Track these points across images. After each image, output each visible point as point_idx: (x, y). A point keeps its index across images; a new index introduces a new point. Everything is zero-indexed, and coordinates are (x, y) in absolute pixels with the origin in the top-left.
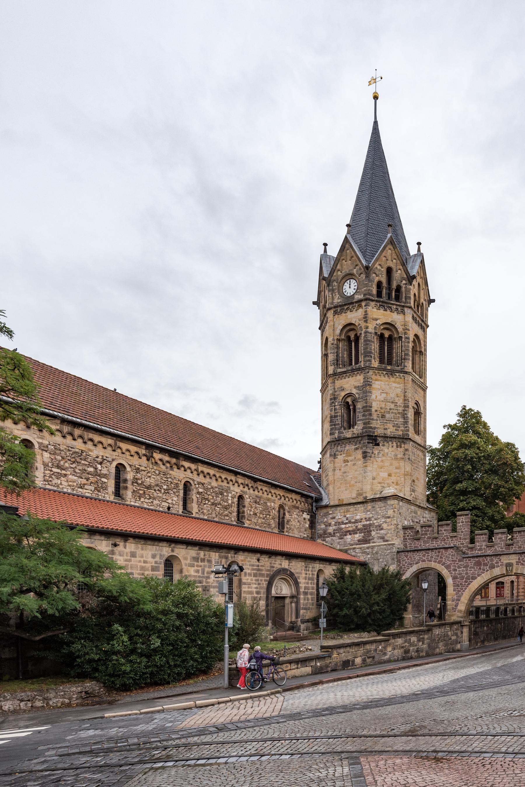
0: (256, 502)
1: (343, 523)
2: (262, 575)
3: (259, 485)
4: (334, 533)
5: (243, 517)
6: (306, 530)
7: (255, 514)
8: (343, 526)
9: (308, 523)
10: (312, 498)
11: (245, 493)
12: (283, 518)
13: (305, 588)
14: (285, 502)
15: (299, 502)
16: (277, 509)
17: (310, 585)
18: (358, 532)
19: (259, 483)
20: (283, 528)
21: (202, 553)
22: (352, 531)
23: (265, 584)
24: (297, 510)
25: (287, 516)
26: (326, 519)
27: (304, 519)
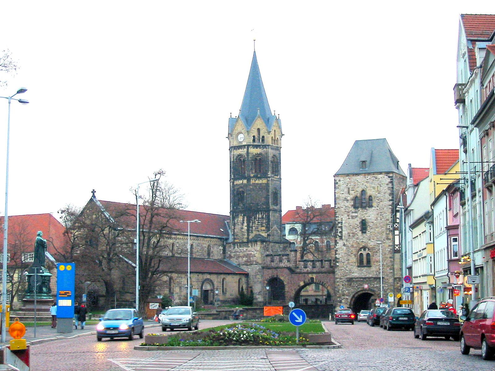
0: (198, 246)
2: (200, 282)
3: (199, 238)
5: (193, 253)
6: (221, 255)
7: (197, 251)
8: (238, 253)
9: (222, 251)
10: (224, 239)
11: (193, 243)
12: (210, 251)
13: (217, 286)
14: (211, 243)
15: (217, 242)
16: (207, 247)
17: (219, 285)
19: (199, 237)
20: (210, 255)
21: (179, 275)
23: (200, 285)
24: (217, 246)
25: (212, 249)
27: (220, 249)
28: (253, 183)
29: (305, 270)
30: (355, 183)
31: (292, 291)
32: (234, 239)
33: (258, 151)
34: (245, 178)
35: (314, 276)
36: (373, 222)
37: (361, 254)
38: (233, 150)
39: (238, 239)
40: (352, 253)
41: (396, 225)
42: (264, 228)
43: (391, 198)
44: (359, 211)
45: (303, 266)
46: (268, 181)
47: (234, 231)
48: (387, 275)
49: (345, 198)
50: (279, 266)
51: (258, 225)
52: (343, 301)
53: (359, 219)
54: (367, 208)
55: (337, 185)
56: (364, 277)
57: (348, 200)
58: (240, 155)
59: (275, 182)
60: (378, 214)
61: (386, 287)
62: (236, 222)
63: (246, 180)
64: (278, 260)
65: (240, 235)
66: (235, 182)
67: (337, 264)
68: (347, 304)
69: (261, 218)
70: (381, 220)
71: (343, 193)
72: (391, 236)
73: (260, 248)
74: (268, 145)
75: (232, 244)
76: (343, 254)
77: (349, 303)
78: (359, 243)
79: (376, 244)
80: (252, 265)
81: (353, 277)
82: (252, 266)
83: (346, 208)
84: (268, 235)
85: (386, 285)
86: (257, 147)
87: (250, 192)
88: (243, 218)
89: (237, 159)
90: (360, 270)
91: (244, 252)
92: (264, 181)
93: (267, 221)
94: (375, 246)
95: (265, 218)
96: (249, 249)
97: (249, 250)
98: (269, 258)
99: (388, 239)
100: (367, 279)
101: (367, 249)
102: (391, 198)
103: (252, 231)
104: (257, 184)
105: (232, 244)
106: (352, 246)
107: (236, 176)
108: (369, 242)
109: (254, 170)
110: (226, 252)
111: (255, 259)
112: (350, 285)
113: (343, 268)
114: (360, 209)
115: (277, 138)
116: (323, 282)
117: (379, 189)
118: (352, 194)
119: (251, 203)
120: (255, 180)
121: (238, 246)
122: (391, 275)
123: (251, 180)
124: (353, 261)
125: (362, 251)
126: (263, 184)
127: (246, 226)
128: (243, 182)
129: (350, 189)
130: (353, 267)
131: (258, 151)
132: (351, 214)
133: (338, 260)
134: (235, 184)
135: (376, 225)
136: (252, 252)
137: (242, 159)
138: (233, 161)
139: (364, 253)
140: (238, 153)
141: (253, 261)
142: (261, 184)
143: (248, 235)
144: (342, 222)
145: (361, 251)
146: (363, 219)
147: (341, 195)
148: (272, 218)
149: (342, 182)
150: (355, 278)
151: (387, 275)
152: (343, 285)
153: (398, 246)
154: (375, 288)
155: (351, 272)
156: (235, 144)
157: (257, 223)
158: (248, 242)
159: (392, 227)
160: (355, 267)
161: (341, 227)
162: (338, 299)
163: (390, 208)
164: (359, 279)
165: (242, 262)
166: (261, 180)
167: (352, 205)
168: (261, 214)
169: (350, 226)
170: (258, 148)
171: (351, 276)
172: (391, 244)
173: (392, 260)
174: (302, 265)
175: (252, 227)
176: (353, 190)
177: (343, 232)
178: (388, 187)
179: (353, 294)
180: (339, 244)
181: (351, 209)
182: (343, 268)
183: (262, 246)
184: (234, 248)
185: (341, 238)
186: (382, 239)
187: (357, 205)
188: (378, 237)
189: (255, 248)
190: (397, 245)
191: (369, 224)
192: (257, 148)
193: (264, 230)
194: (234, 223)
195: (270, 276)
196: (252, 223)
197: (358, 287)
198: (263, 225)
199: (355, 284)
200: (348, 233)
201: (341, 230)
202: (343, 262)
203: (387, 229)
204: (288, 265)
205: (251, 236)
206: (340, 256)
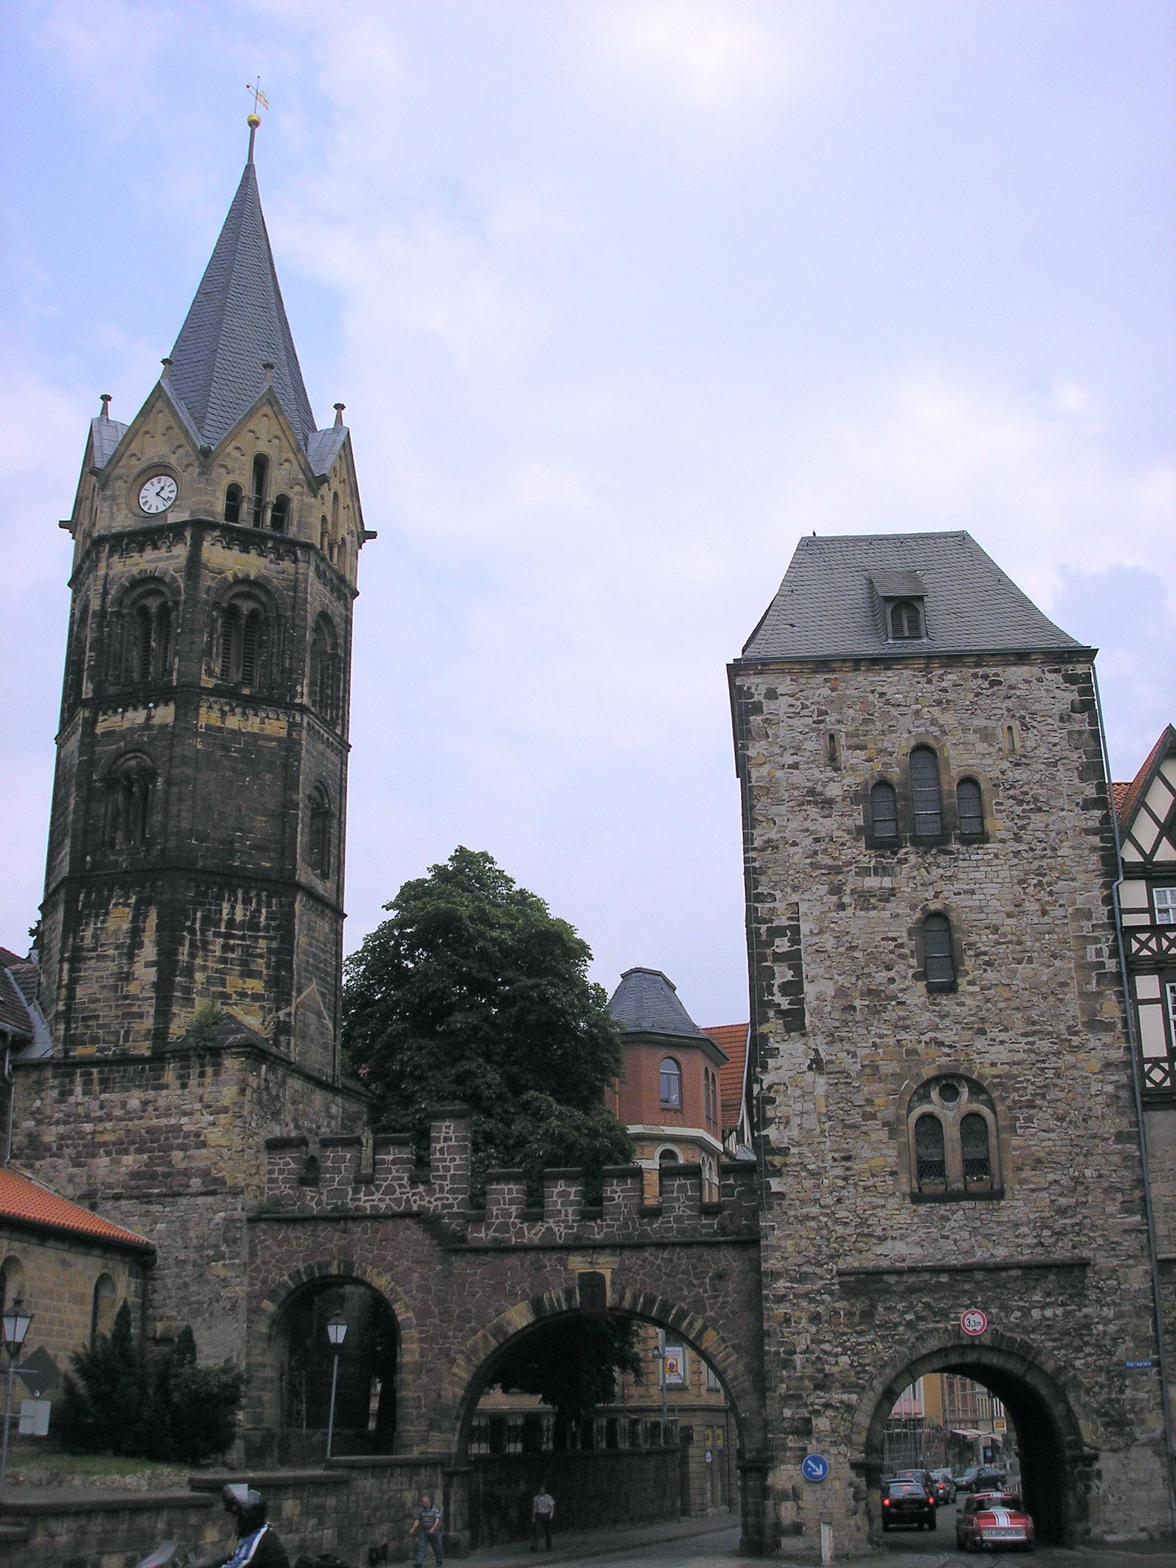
1: (88, 1118)
4: (60, 1148)
8: (88, 1127)
18: (132, 1148)
22: (114, 1144)
26: (38, 1103)
28: (208, 727)
29: (533, 1234)
30: (866, 707)
31: (453, 1362)
32: (71, 1041)
33: (251, 564)
34: (164, 695)
35: (606, 1266)
36: (996, 930)
37: (929, 1125)
38: (104, 555)
39: (94, 1040)
40: (873, 1117)
41: (1144, 945)
42: (256, 986)
43: (1090, 791)
44: (900, 862)
45: (513, 1209)
46: (292, 725)
47: (71, 996)
48: (1111, 1247)
49: (811, 792)
50: (351, 1205)
51: (224, 960)
52: (822, 1423)
53: (904, 910)
54: (955, 846)
55: (756, 720)
56: (952, 1261)
57: (829, 803)
58: (148, 583)
59: (321, 747)
60: (1023, 881)
61: (1106, 1321)
62: (88, 942)
63: (172, 707)
64: (346, 1170)
65: (107, 1013)
66: (101, 718)
67: (776, 1185)
68: (848, 1440)
69: (242, 926)
70: (1044, 913)
71: (789, 759)
72: (1110, 1009)
73: (242, 1092)
74: (308, 547)
75: (49, 1073)
76: (811, 1122)
77: (860, 1438)
78: (912, 1052)
79: (1022, 1056)
80: (179, 1195)
81: (885, 1263)
82: (183, 1201)
83: (817, 847)
84: (283, 1029)
85: (1108, 1312)
86: (245, 540)
87: (188, 771)
88: (139, 915)
89: (127, 602)
90: (927, 1220)
91: (129, 1116)
92: (274, 726)
93: (274, 945)
94: (1015, 1070)
95: (267, 928)
96: (169, 1096)
97: (162, 1102)
98: (289, 1161)
99: (1094, 1024)
100: (979, 1276)
101: (965, 1092)
102: (1090, 791)
103: (188, 991)
104: (233, 732)
105: (49, 1073)
106: (872, 1070)
107: (112, 690)
108: (980, 1043)
109: (220, 661)
110: (12, 1116)
111: (201, 1158)
112: (868, 1315)
113: (815, 1210)
114: (906, 850)
115: (343, 539)
116: (665, 1308)
117: (1018, 745)
118: (853, 769)
119: (191, 833)
120: (224, 714)
121: (88, 1083)
122: (1130, 1243)
123: (203, 710)
124: (880, 1162)
125: (935, 1104)
126: (269, 738)
127: (148, 965)
128: (149, 717)
129: (843, 740)
130: (882, 1202)
131: (251, 564)
132: (852, 881)
133: (777, 1160)
134: (100, 729)
135: (1019, 943)
136: (184, 1120)
137: (153, 604)
138: (102, 614)
139: (950, 1114)
140: (135, 571)
141: (187, 1173)
142: (255, 734)
143: (163, 1014)
144: (796, 930)
145: (925, 1098)
146: (934, 906)
147: (779, 774)
148: (301, 940)
149: (791, 700)
150: (899, 1272)
151: (1111, 1247)
152: (815, 1318)
153: (1166, 1065)
154: (1034, 1330)
155: (871, 1235)
156: (122, 522)
157: (217, 946)
158: (158, 1059)
159: (1114, 953)
160: (893, 1203)
161: (793, 959)
162: (787, 1413)
163: (1093, 849)
164: (926, 1277)
165: (112, 1179)
166: (256, 715)
167: (859, 829)
168: (247, 901)
169: (853, 948)
170: (253, 552)
171: (870, 1255)
172: (1117, 1054)
173: (1131, 1148)
174: (512, 1202)
175: (189, 971)
176: (863, 748)
177: (807, 987)
178: (1070, 733)
179: (890, 1372)
180: (781, 1061)
181: (847, 854)
182: (815, 1210)
183: (253, 1082)
184: (65, 1094)
185: (794, 1021)
186: (1062, 1027)
187: (885, 831)
188: (1034, 1015)
189: (208, 1092)
190: (1156, 1062)
191: (974, 938)
192: (245, 550)
193: (256, 997)
194: (77, 949)
195: (301, 1266)
196: (193, 945)
197: (922, 1325)
198: (253, 967)
199: (887, 1311)
200: (841, 992)
201: (789, 975)
202: (812, 1174)
203: (1084, 967)
204: (419, 1198)
205: (181, 1024)
206: (795, 1133)
